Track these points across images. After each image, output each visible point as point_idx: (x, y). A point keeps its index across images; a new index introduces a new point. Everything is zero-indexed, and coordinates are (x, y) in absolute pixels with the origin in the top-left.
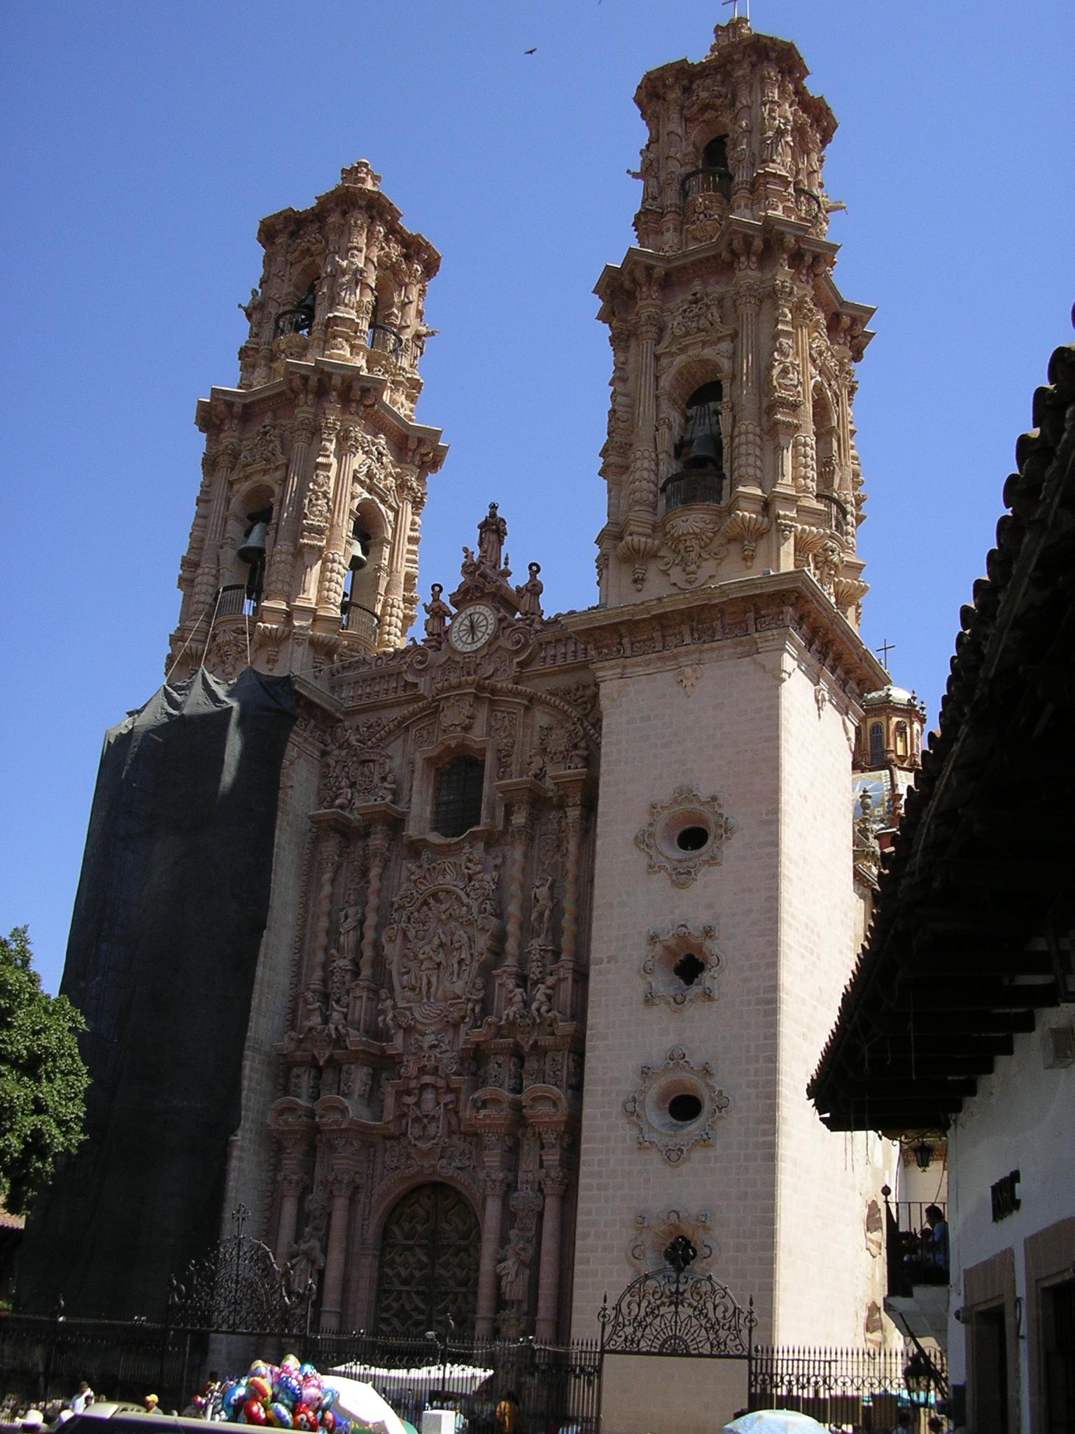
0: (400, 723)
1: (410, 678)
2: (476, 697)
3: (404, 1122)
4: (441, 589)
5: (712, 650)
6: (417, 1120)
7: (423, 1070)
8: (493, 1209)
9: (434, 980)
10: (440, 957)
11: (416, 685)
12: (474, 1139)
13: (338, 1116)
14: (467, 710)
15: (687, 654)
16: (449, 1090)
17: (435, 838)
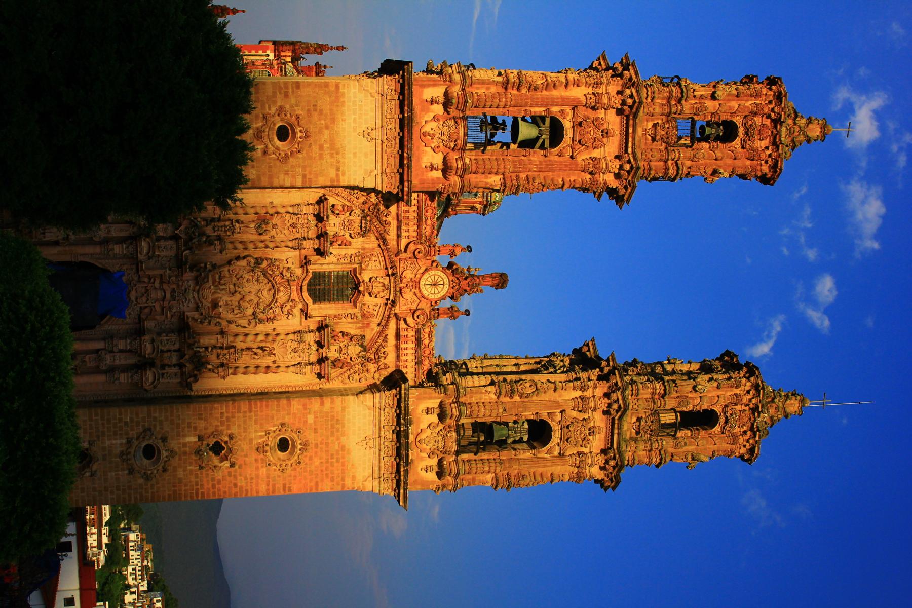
0: (384, 241)
1: (412, 247)
2: (387, 300)
3: (146, 280)
4: (470, 251)
5: (380, 455)
6: (147, 291)
7: (173, 291)
8: (100, 345)
9: (224, 292)
10: (237, 297)
11: (405, 251)
12: (137, 321)
13: (145, 250)
14: (382, 294)
15: (380, 444)
16: (163, 308)
17: (310, 275)
